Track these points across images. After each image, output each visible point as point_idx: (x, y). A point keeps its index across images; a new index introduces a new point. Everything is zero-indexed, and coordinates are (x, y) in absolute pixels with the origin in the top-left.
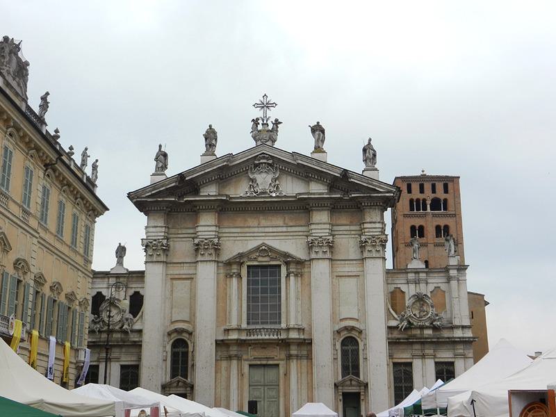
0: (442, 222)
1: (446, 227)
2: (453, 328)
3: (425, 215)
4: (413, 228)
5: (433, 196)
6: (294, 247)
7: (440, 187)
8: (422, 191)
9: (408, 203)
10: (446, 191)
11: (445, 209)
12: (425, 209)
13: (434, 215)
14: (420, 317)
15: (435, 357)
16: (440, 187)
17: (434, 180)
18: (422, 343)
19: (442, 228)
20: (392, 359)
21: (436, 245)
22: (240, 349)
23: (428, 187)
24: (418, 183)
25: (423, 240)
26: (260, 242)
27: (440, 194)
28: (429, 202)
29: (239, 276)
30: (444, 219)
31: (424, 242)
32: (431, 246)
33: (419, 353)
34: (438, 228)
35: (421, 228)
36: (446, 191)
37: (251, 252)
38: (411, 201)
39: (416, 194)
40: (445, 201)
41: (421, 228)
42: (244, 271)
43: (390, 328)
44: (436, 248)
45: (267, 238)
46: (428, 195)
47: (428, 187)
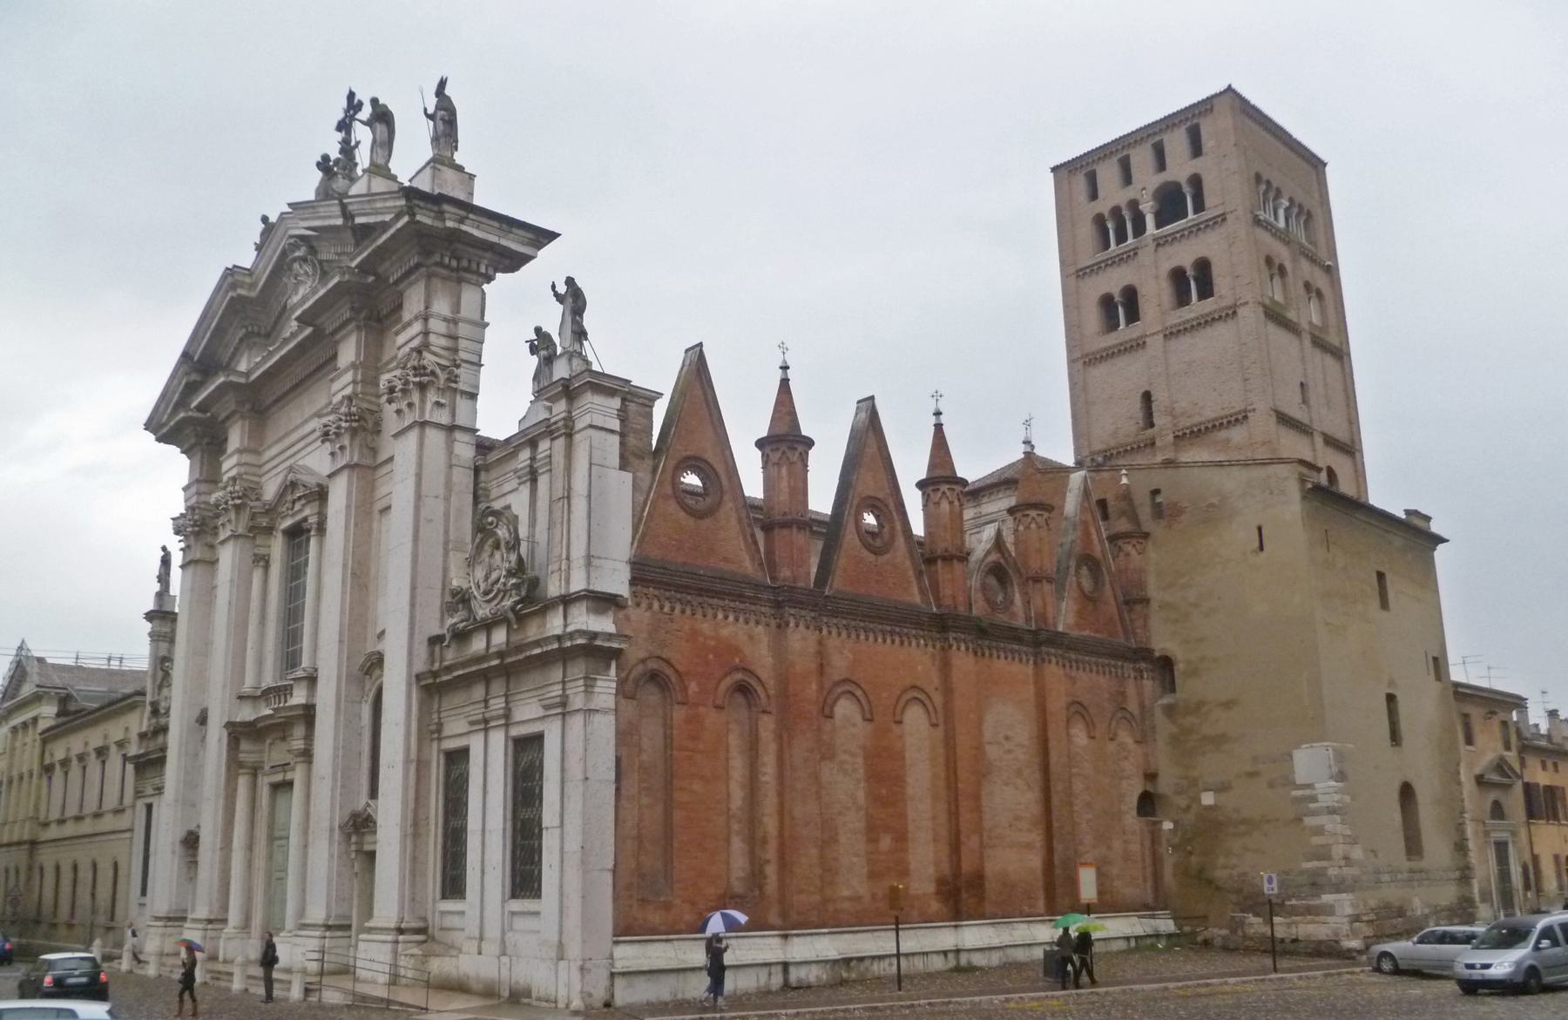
0: (1184, 256)
1: (1203, 266)
2: (548, 606)
3: (1135, 252)
4: (1107, 302)
5: (1157, 180)
6: (318, 461)
7: (1176, 144)
8: (1127, 179)
9: (1087, 231)
10: (1197, 150)
11: (1199, 207)
12: (1140, 229)
13: (1160, 243)
14: (486, 593)
15: (507, 715)
16: (1176, 144)
17: (1153, 136)
18: (486, 677)
19: (1190, 273)
20: (440, 739)
21: (1171, 334)
22: (256, 748)
23: (1142, 159)
24: (1115, 159)
25: (1136, 330)
26: (288, 463)
27: (1180, 168)
28: (1148, 208)
29: (263, 561)
30: (1193, 240)
31: (1134, 336)
32: (1155, 343)
33: (477, 712)
34: (1178, 276)
35: (1131, 296)
36: (1197, 150)
37: (281, 495)
38: (1099, 221)
39: (1113, 194)
40: (1196, 182)
41: (1131, 296)
42: (277, 548)
43: (435, 641)
44: (1174, 344)
45: (309, 449)
46: (1147, 182)
47: (1142, 159)
